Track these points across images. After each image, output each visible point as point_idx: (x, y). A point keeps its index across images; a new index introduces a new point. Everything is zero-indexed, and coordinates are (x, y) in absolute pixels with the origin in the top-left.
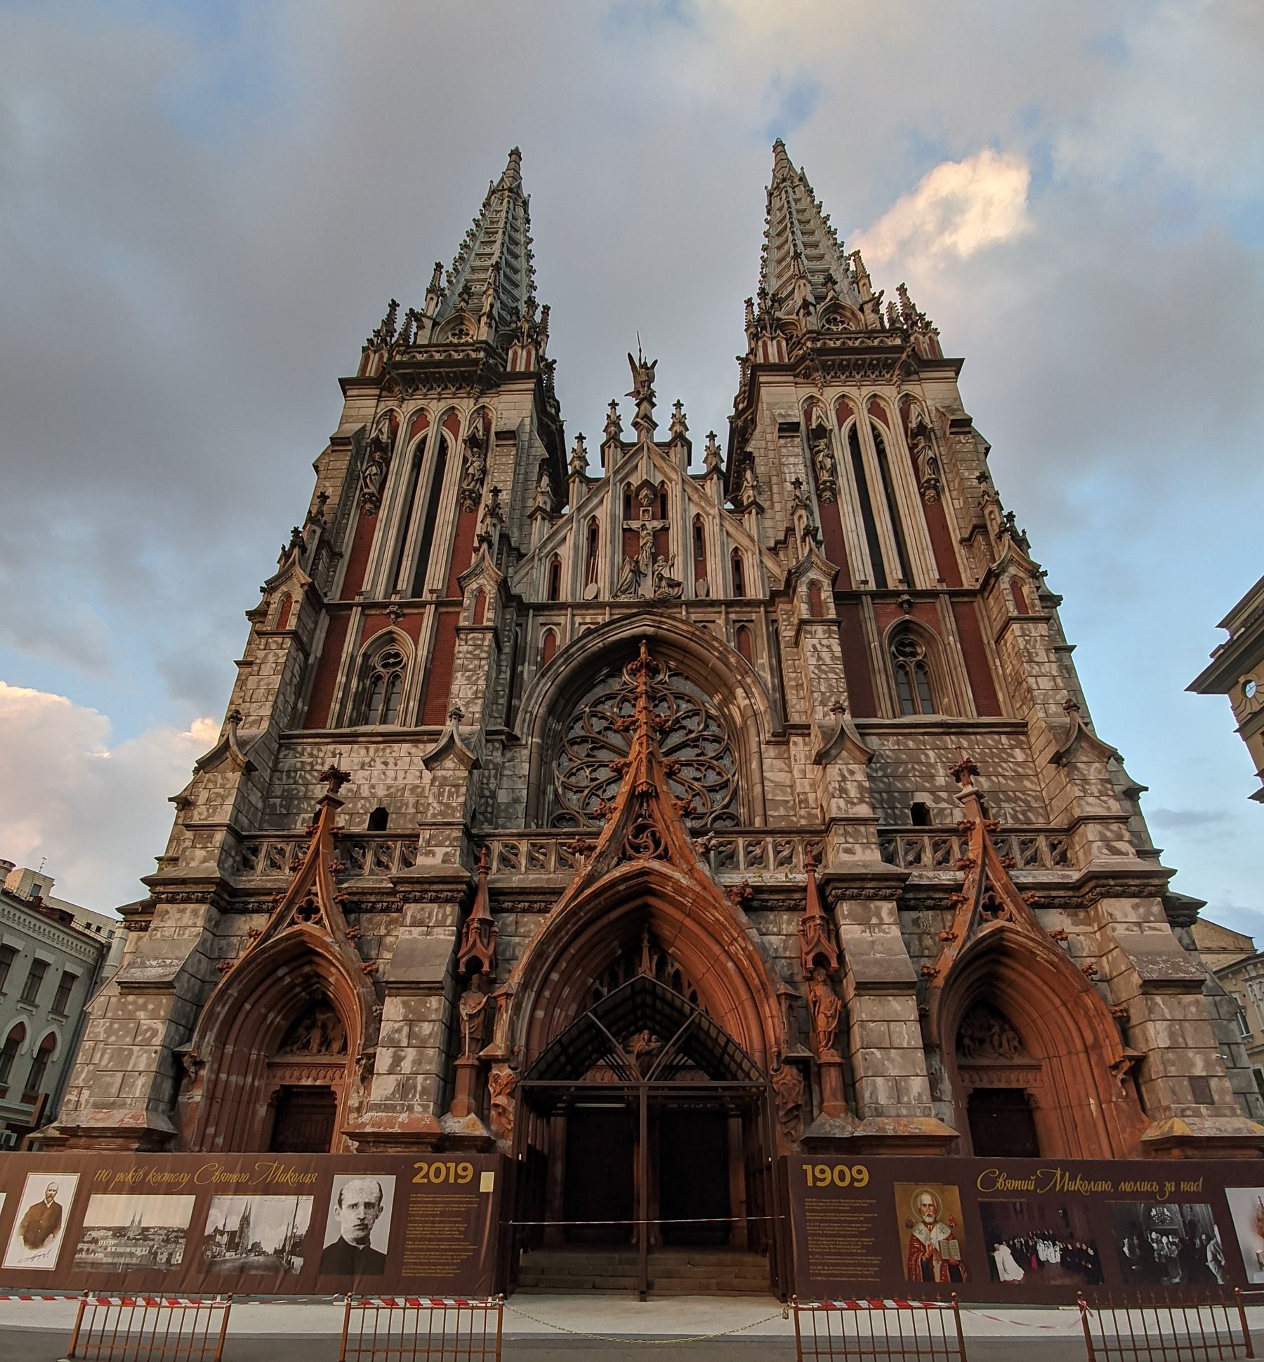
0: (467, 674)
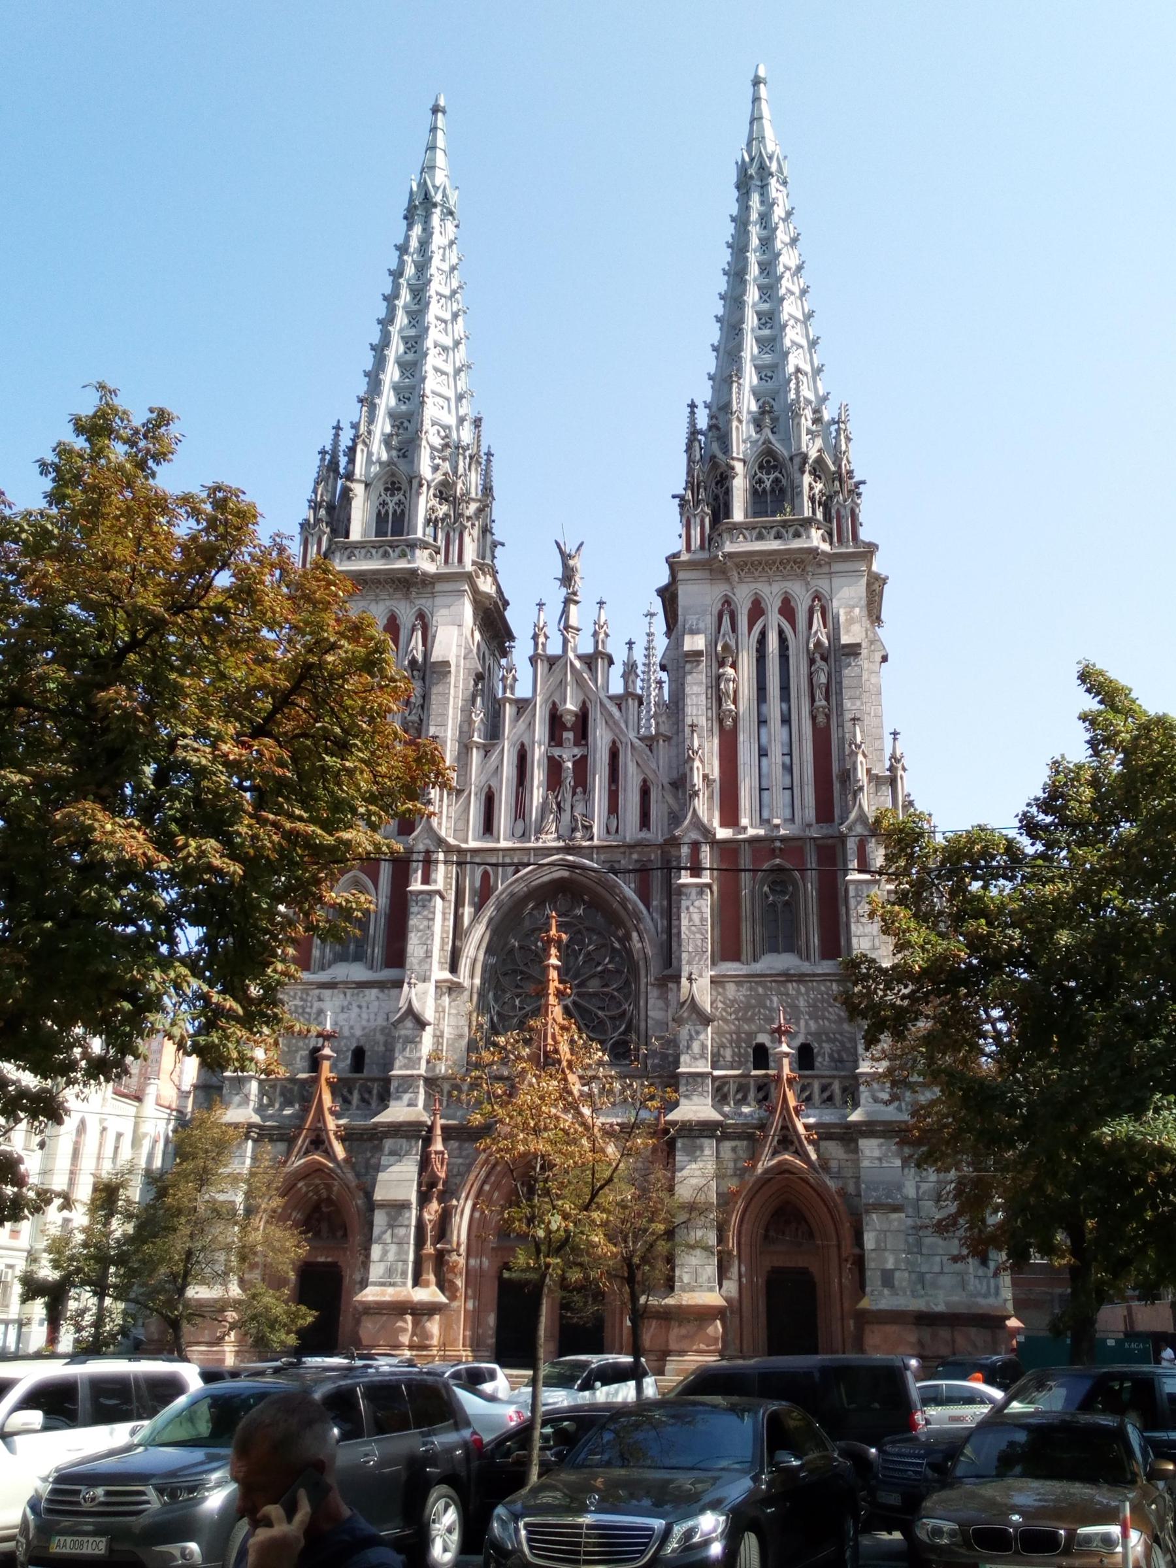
0: (419, 934)
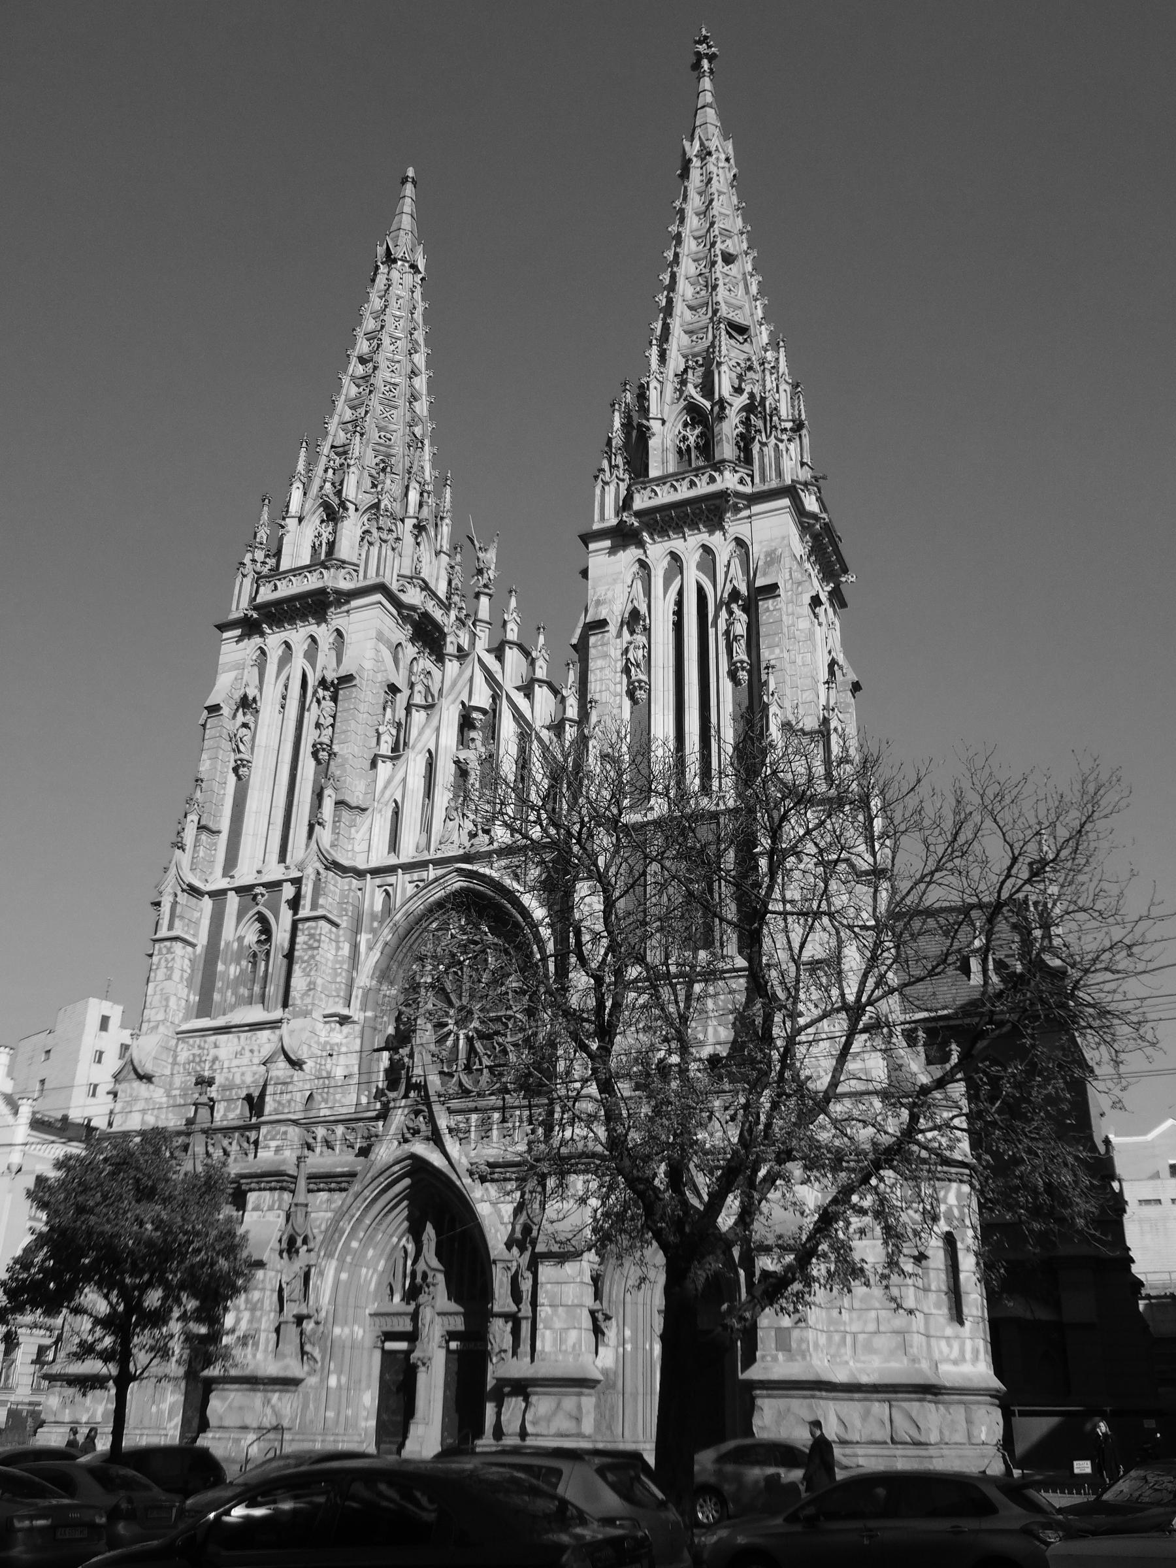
0: (304, 965)
